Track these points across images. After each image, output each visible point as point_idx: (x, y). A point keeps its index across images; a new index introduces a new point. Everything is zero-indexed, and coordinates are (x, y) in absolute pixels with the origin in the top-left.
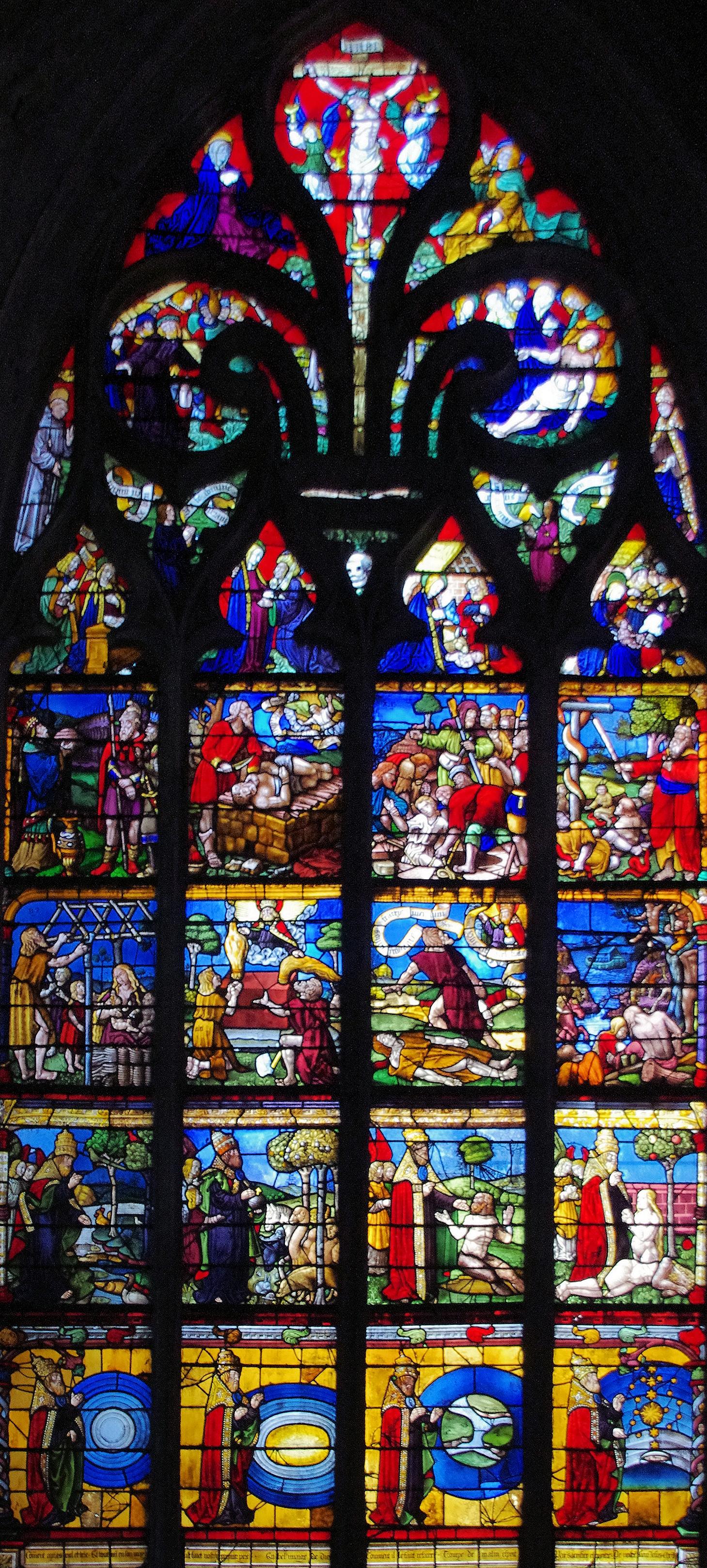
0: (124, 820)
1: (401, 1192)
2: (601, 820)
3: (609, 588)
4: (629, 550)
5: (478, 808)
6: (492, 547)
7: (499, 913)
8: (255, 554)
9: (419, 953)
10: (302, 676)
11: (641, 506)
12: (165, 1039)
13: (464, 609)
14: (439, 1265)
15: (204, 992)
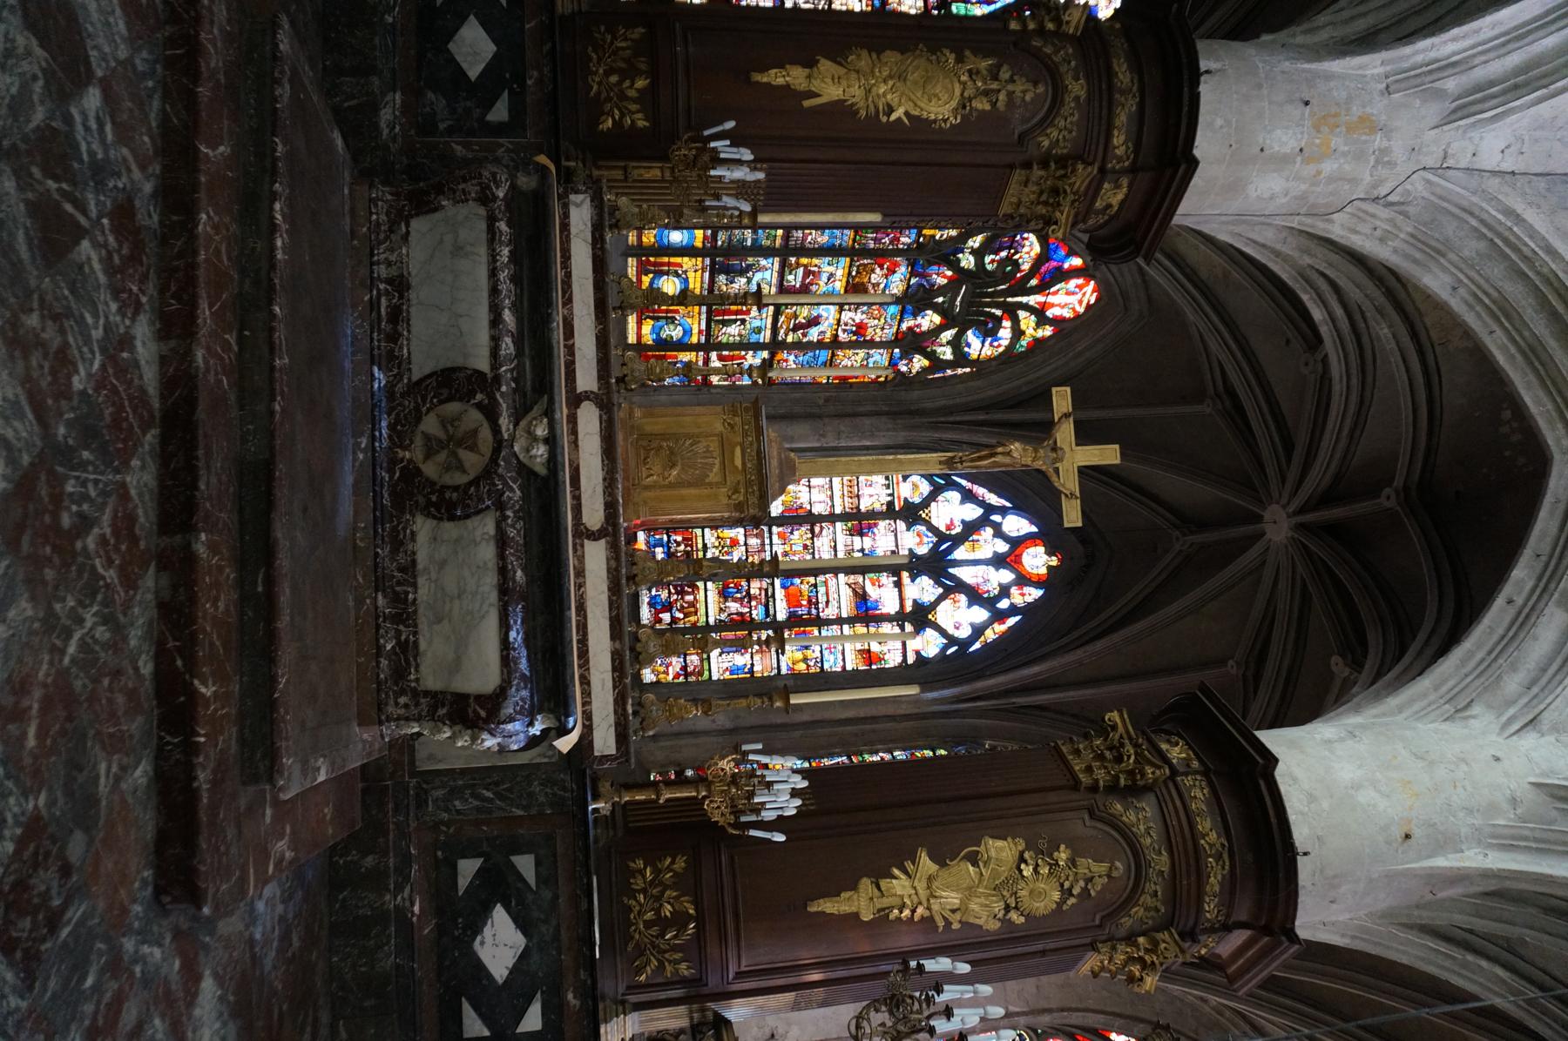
0: (875, 239)
1: (748, 312)
2: (850, 360)
3: (917, 358)
4: (926, 363)
5: (860, 328)
6: (937, 331)
7: (828, 335)
8: (949, 273)
9: (819, 316)
10: (909, 286)
11: (937, 363)
12: (803, 251)
13: (919, 326)
14: (726, 323)
15: (815, 261)
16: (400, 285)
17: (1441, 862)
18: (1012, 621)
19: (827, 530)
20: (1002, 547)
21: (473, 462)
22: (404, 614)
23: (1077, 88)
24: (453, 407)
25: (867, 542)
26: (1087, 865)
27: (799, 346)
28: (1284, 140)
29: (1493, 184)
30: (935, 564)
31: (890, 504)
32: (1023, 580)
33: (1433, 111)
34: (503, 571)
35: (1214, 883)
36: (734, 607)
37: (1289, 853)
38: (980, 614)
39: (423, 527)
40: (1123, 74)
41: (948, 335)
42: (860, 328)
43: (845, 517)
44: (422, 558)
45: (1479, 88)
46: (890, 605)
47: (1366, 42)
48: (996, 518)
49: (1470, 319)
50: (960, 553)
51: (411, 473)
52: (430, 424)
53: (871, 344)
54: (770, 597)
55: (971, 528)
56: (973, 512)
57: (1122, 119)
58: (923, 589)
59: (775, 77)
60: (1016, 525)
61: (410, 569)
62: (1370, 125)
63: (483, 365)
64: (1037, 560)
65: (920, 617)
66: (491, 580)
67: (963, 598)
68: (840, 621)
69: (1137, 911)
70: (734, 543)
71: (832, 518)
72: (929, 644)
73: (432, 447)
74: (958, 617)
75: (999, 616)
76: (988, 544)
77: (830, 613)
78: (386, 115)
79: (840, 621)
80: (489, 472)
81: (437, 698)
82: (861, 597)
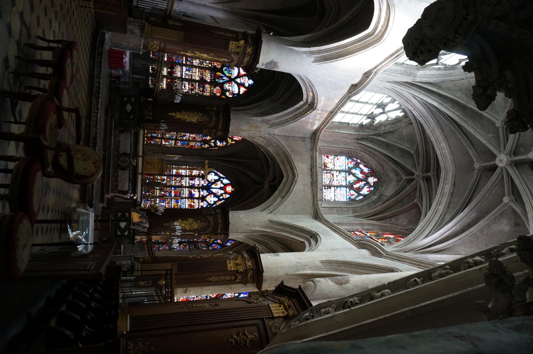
6: (210, 140)
16: (119, 142)
17: (252, 229)
18: (223, 201)
19: (185, 178)
20: (222, 186)
21: (127, 164)
22: (117, 181)
23: (214, 119)
24: (125, 157)
25: (193, 182)
26: (202, 223)
27: (181, 140)
28: (245, 128)
29: (277, 136)
30: (207, 188)
31: (199, 174)
32: (226, 193)
33: (267, 126)
34: (129, 177)
35: (220, 227)
36: (163, 193)
37: (229, 223)
38: (216, 199)
39: (120, 171)
40: (221, 118)
41: (213, 141)
42: (194, 138)
43: (188, 176)
44: (120, 174)
45: (274, 123)
46: (197, 195)
47: (257, 115)
48: (222, 179)
49: (274, 155)
50: (213, 186)
51: (119, 164)
52: (122, 159)
53: (197, 141)
54: (170, 193)
55: (216, 181)
56: (216, 178)
57: (220, 123)
58: (204, 193)
59: (171, 114)
60: (226, 181)
61: (118, 176)
62: (257, 127)
63: (129, 153)
64: (229, 189)
65: (203, 199)
66: (128, 178)
67: (213, 196)
68: (186, 198)
69: (209, 230)
70: (164, 179)
71: (186, 176)
72: (204, 204)
73: (122, 162)
74: (211, 199)
75: (220, 200)
76: (219, 185)
77: (184, 196)
78: (116, 116)
79: (186, 198)
80: (129, 165)
81: (120, 191)
82: (190, 193)
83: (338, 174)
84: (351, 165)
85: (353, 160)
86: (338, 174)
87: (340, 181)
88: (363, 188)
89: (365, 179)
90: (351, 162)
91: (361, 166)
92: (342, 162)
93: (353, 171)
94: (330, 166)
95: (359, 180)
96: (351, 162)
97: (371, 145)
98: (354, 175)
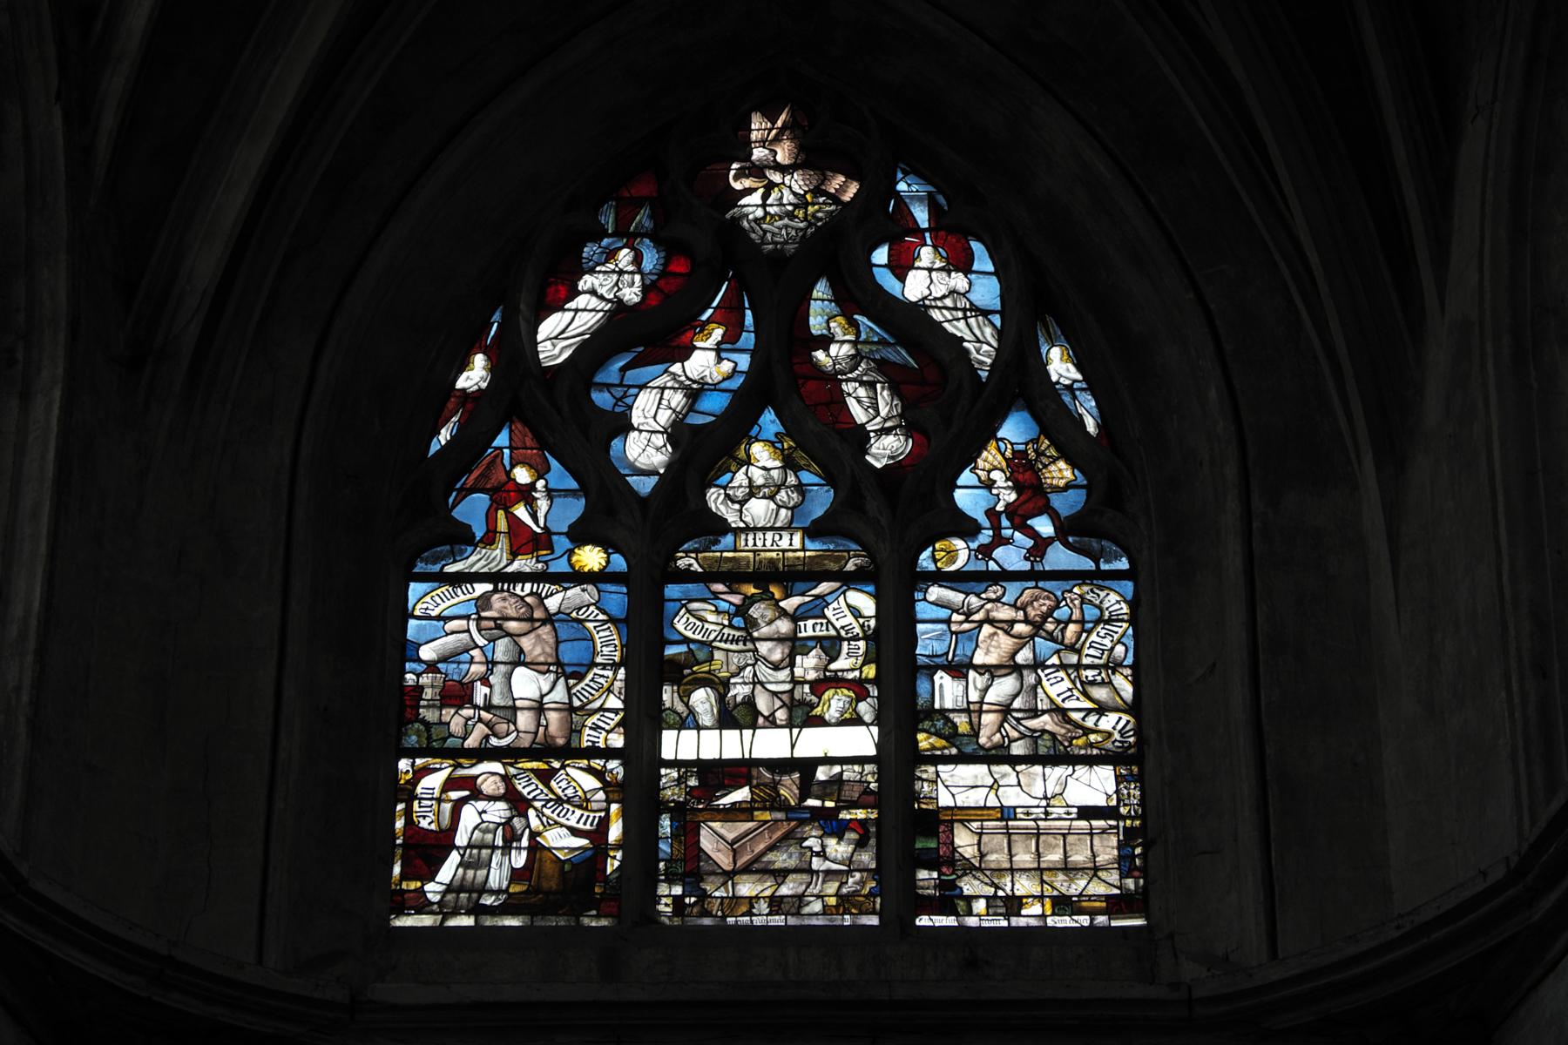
83: (702, 699)
84: (550, 506)
85: (470, 446)
86: (702, 699)
87: (808, 665)
88: (911, 323)
89: (766, 284)
90: (506, 494)
91: (558, 335)
92: (496, 639)
93: (645, 450)
94: (569, 818)
95: (784, 382)
96: (506, 494)
97: (249, 160)
98: (704, 448)
